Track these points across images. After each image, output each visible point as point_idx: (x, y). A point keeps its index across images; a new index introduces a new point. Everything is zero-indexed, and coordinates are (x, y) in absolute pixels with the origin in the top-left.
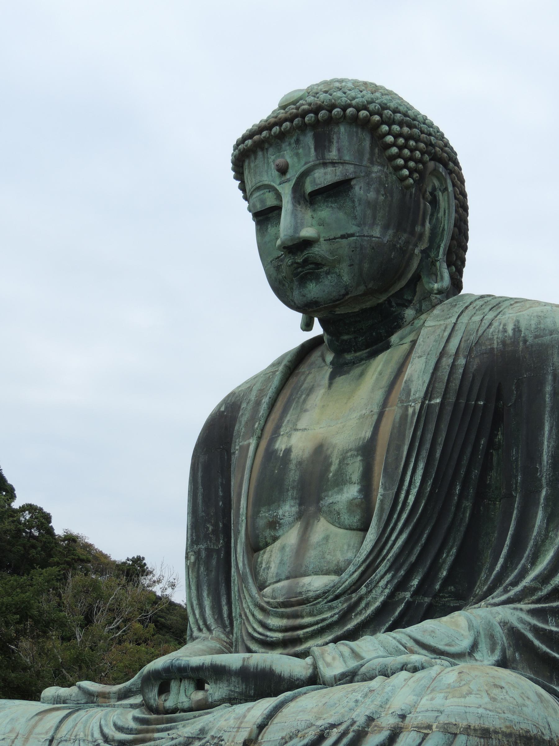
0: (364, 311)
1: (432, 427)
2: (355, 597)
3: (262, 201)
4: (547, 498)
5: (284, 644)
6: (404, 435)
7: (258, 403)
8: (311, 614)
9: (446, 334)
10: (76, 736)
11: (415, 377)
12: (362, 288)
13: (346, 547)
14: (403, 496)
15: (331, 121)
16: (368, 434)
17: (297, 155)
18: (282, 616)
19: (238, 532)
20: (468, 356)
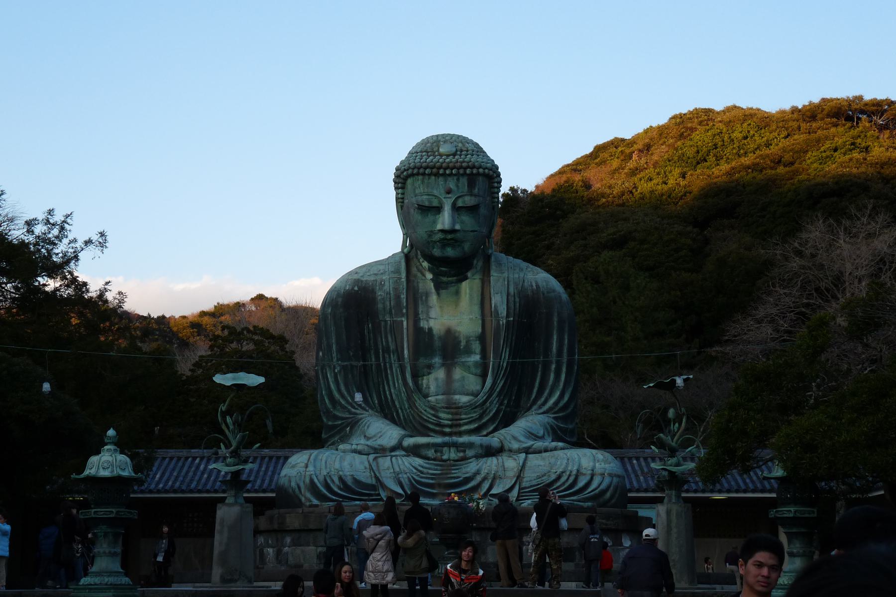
4: (556, 368)
5: (451, 426)
7: (398, 297)
15: (478, 174)
16: (480, 330)
17: (457, 186)
18: (448, 413)
19: (405, 367)
20: (519, 297)
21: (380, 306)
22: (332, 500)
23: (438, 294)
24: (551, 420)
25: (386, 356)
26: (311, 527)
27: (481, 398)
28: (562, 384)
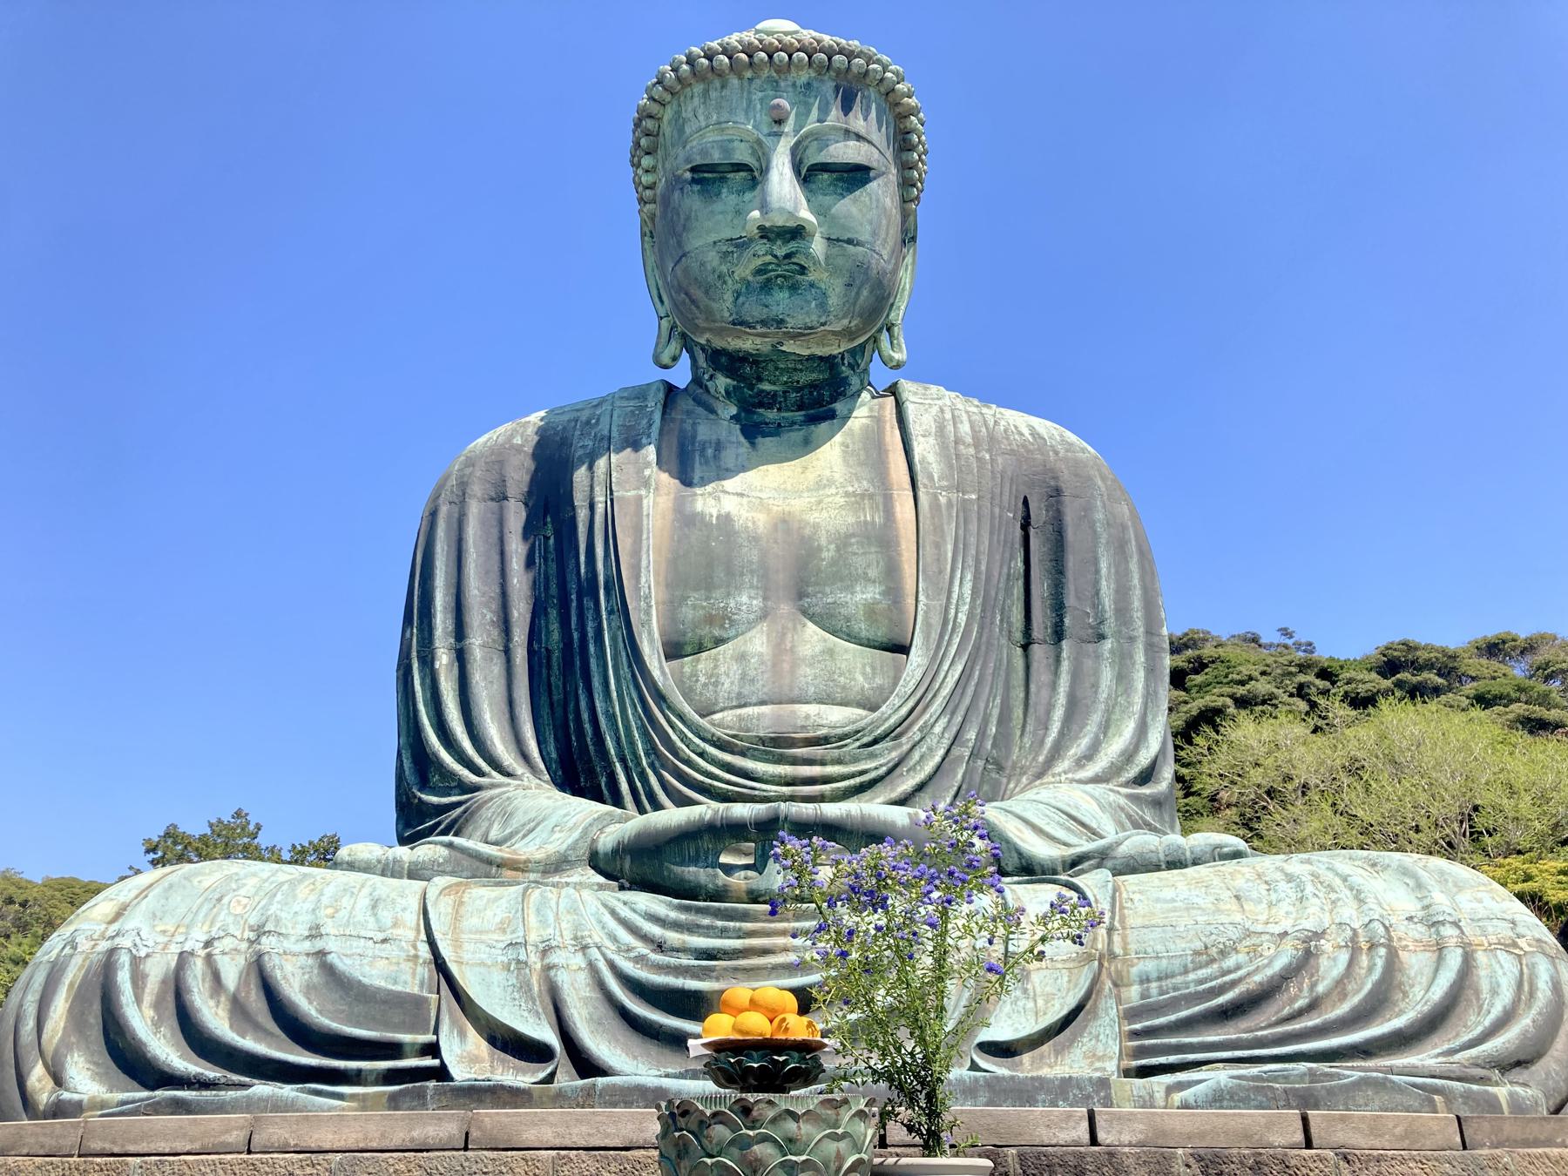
0: (811, 358)
1: (973, 527)
3: (725, 148)
6: (943, 531)
8: (839, 762)
9: (948, 416)
10: (575, 938)
11: (931, 458)
12: (845, 322)
13: (868, 669)
14: (953, 612)
18: (780, 760)
20: (989, 451)
23: (753, 444)
24: (1123, 801)
25: (588, 603)
27: (891, 712)
28: (1138, 700)
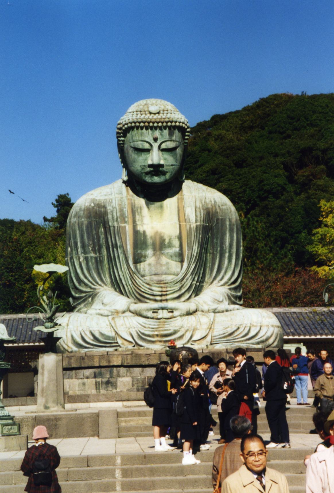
1: (198, 232)
2: (183, 283)
3: (143, 146)
5: (161, 296)
7: (121, 210)
8: (170, 287)
17: (161, 135)
18: (159, 287)
20: (203, 209)
21: (110, 216)
22: (86, 348)
23: (148, 208)
25: (115, 250)
26: (74, 365)
27: (180, 276)
